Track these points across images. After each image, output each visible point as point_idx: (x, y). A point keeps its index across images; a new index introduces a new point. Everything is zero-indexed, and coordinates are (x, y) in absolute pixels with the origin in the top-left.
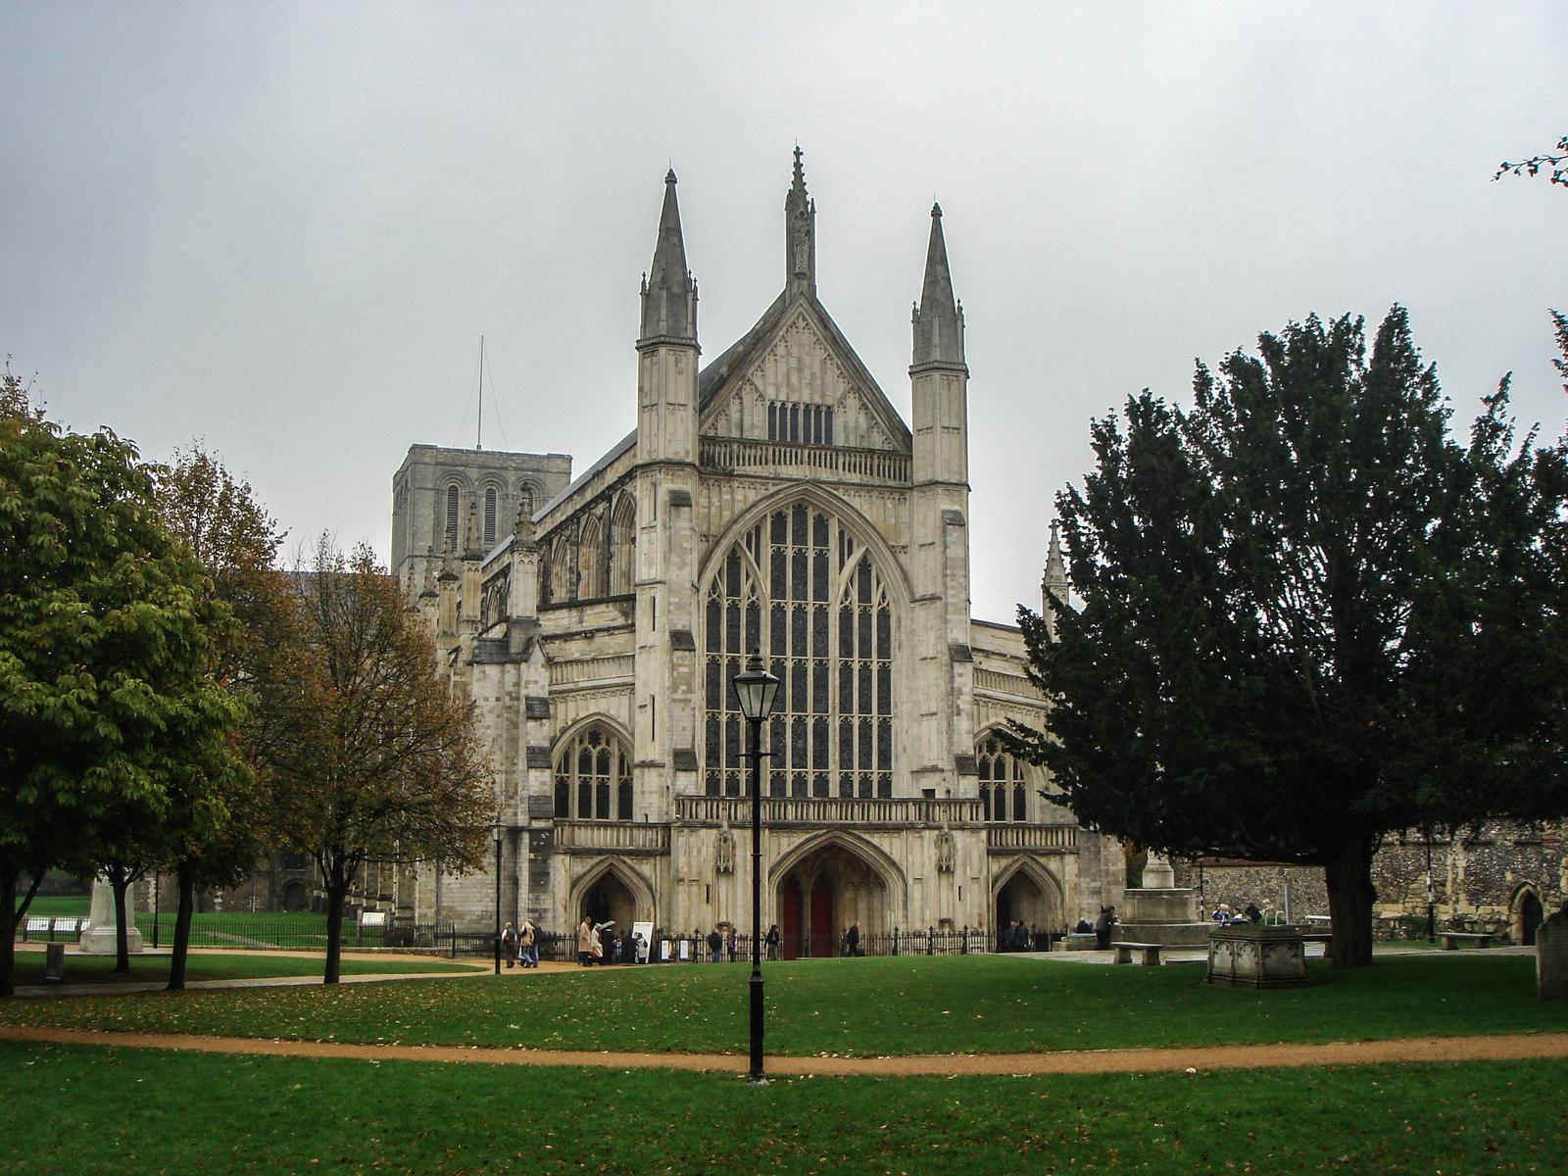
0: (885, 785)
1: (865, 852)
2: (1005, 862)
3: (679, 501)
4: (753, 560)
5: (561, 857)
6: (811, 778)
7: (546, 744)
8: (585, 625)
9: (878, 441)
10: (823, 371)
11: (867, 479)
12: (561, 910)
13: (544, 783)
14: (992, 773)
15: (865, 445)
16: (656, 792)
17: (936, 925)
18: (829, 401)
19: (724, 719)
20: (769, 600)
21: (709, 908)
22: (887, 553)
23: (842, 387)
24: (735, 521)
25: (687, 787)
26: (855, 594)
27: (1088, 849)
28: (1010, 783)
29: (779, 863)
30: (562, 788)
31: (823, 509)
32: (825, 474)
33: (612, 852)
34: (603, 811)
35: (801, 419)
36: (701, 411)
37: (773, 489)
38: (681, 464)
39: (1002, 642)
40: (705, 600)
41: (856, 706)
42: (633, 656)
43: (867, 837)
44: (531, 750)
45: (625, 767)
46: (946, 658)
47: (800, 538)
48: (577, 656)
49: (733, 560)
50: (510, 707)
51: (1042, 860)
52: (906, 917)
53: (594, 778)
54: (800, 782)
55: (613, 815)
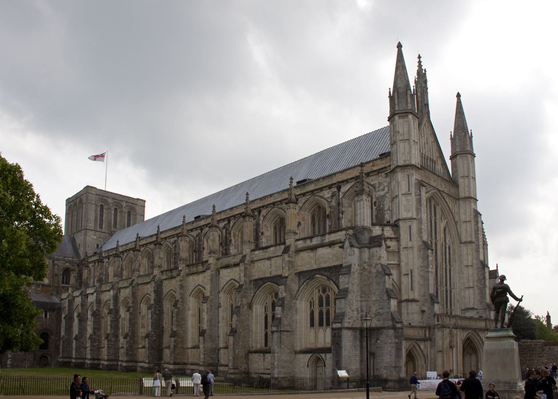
16: (416, 313)
31: (436, 201)
42: (399, 252)
50: (367, 269)
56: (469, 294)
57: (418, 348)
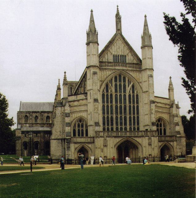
0: (138, 129)
1: (134, 142)
2: (162, 143)
3: (95, 73)
4: (111, 85)
5: (73, 144)
6: (123, 128)
7: (69, 122)
9: (135, 62)
10: (124, 48)
11: (133, 69)
12: (73, 154)
13: (69, 129)
14: (159, 126)
15: (133, 63)
17: (148, 156)
18: (125, 54)
19: (106, 117)
20: (114, 93)
21: (102, 153)
22: (137, 83)
23: (128, 51)
24: (107, 78)
26: (131, 92)
27: (178, 140)
28: (163, 128)
30: (74, 131)
32: (124, 68)
33: (83, 143)
34: (83, 135)
35: (120, 58)
36: (99, 57)
37: (114, 71)
38: (95, 66)
39: (161, 100)
40: (101, 93)
41: (132, 113)
43: (134, 138)
44: (67, 123)
45: (87, 126)
46: (149, 103)
47: (120, 81)
48: (76, 105)
49: (107, 86)
51: (169, 142)
52: (142, 154)
53: (81, 129)
54: (121, 129)
55: (85, 136)
57: (86, 146)
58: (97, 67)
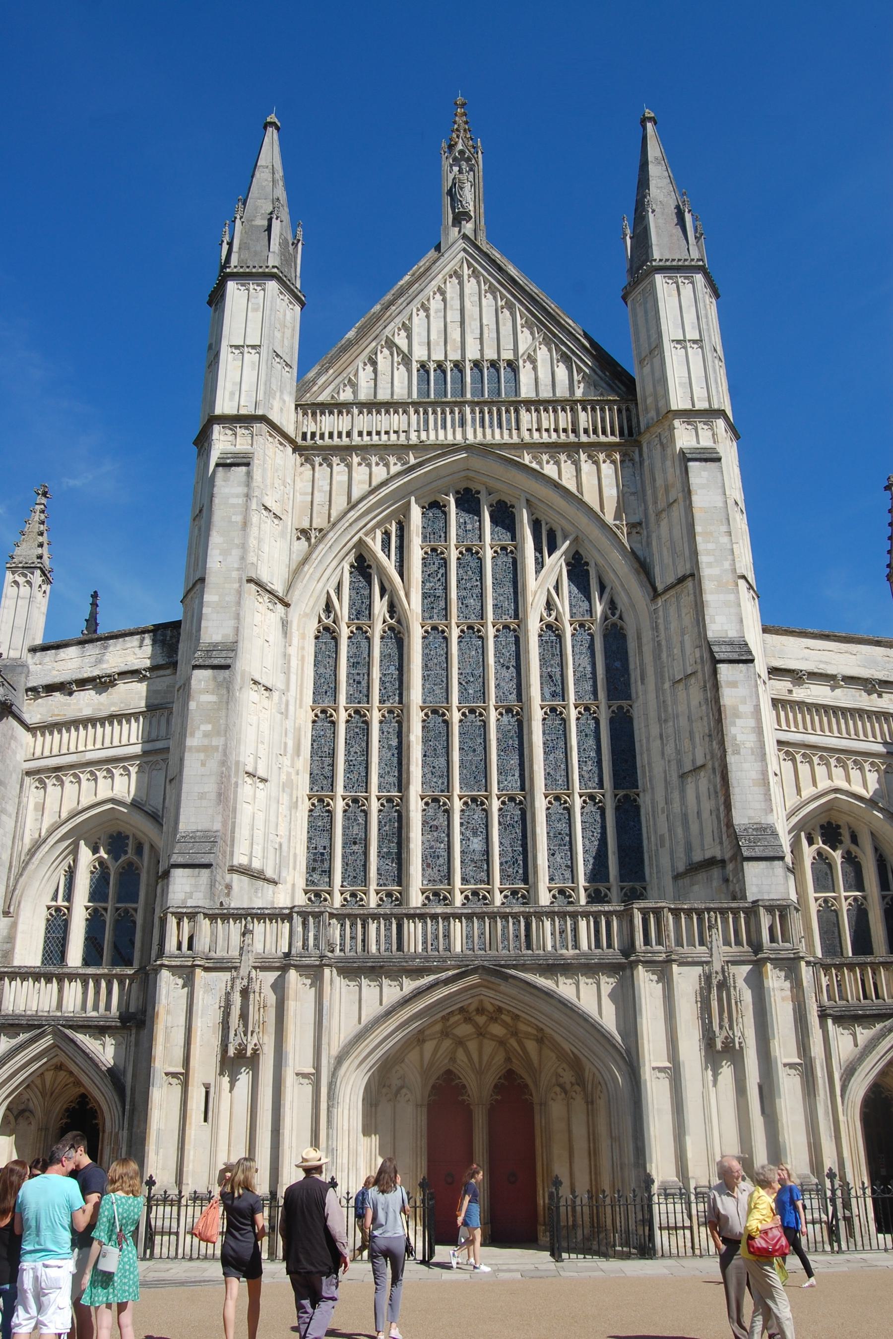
4: (390, 565)
8: (104, 666)
18: (507, 355)
25: (190, 895)
29: (359, 1037)
32: (497, 436)
37: (413, 461)
48: (87, 712)
56: (698, 798)
58: (258, 427)
